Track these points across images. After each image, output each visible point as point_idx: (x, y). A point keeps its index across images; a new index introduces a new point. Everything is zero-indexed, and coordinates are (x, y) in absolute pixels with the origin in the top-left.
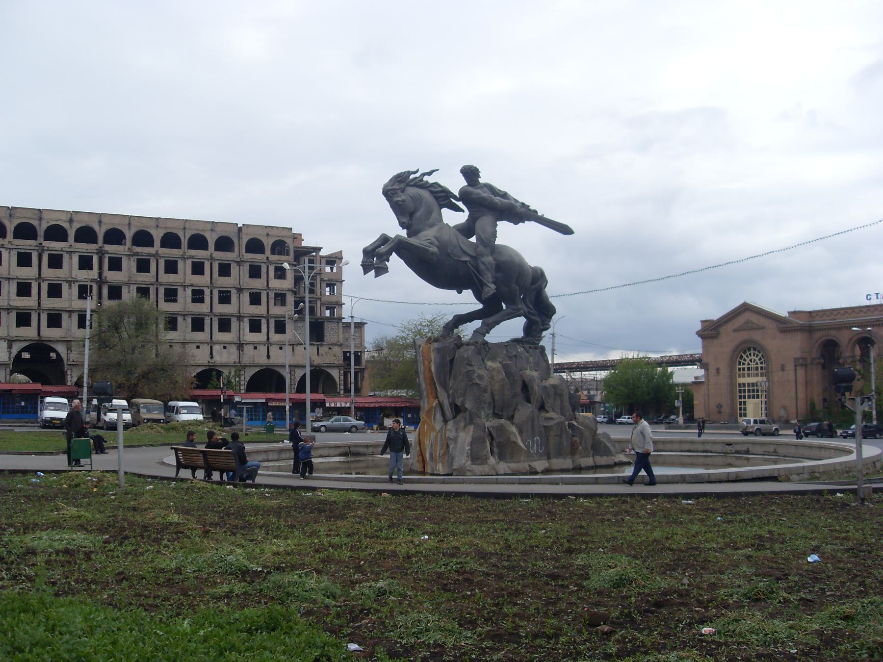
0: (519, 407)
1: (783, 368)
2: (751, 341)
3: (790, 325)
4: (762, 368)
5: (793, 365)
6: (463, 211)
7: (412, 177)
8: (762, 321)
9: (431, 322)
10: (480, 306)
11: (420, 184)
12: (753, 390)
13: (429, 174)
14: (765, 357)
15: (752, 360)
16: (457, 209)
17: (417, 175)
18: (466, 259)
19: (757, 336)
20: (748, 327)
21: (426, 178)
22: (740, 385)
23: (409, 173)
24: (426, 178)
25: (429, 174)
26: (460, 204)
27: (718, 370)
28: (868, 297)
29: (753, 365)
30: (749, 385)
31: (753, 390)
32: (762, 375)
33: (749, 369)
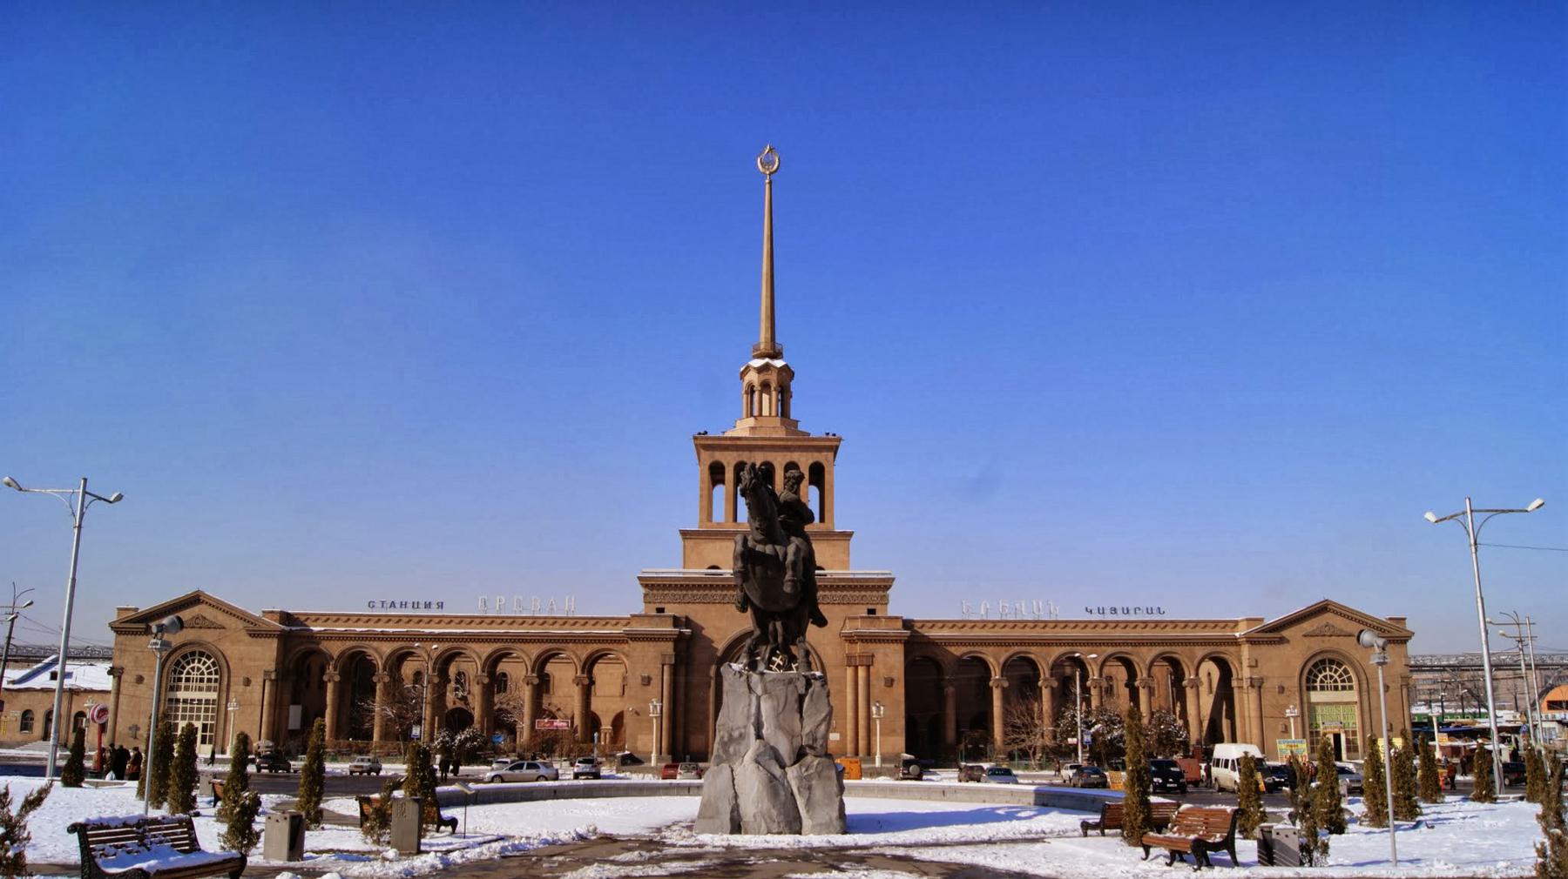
1: (248, 682)
2: (200, 644)
3: (264, 627)
4: (209, 680)
5: (261, 680)
8: (221, 618)
12: (192, 710)
14: (221, 667)
15: (198, 668)
19: (208, 636)
20: (201, 623)
22: (171, 700)
27: (140, 680)
28: (371, 605)
29: (195, 675)
30: (185, 701)
31: (192, 710)
32: (209, 689)
33: (188, 680)
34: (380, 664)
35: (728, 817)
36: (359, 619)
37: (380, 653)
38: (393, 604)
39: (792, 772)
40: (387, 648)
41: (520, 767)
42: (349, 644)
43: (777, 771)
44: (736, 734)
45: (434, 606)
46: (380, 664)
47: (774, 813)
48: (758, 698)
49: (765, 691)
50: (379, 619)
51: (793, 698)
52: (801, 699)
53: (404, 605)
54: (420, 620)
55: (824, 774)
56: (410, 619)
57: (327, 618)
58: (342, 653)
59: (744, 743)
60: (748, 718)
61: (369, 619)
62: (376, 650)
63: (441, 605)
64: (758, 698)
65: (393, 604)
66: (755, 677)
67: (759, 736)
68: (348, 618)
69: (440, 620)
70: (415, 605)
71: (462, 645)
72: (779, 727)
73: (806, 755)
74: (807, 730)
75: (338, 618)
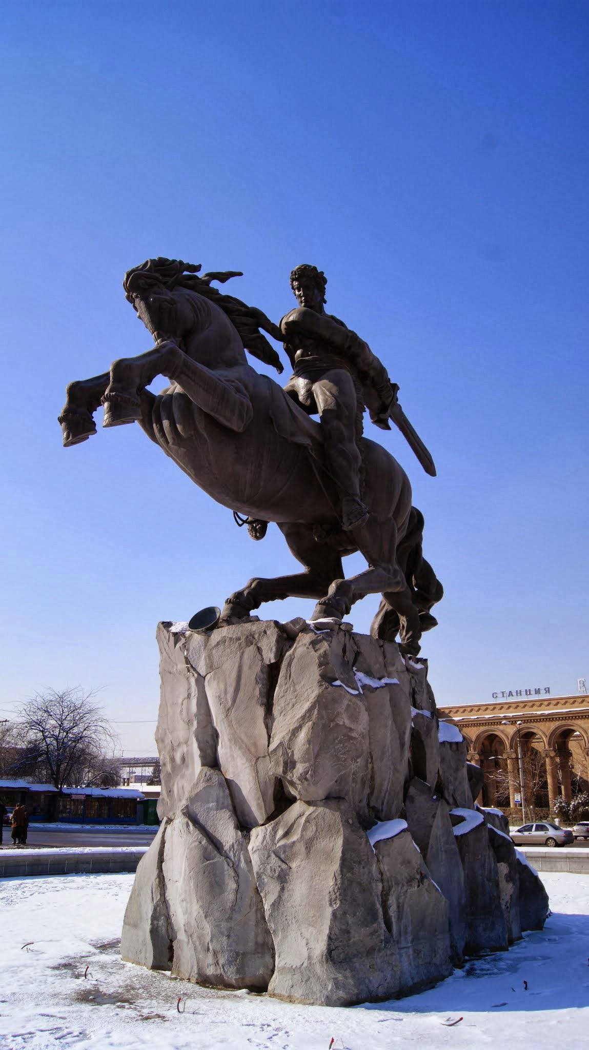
0: (412, 791)
6: (280, 368)
7: (185, 273)
9: (61, 697)
10: (297, 568)
11: (202, 287)
13: (223, 277)
16: (272, 359)
17: (200, 275)
18: (306, 441)
21: (215, 284)
23: (182, 266)
24: (215, 284)
25: (223, 277)
26: (278, 347)
28: (494, 695)
34: (507, 743)
35: (148, 927)
36: (486, 707)
37: (507, 732)
38: (511, 694)
39: (258, 835)
40: (511, 730)
41: (529, 829)
42: (482, 729)
43: (228, 834)
44: (178, 758)
45: (542, 691)
46: (507, 743)
47: (208, 929)
48: (200, 680)
49: (211, 667)
50: (501, 706)
51: (252, 673)
52: (271, 674)
53: (519, 693)
54: (533, 704)
55: (323, 844)
56: (525, 704)
57: (464, 709)
58: (478, 737)
59: (188, 773)
60: (189, 723)
61: (494, 707)
62: (502, 732)
63: (548, 691)
64: (200, 680)
65: (511, 694)
66: (197, 638)
67: (212, 762)
68: (479, 708)
69: (549, 702)
70: (528, 692)
71: (569, 722)
72: (235, 740)
73: (293, 800)
74: (273, 746)
75: (472, 709)
